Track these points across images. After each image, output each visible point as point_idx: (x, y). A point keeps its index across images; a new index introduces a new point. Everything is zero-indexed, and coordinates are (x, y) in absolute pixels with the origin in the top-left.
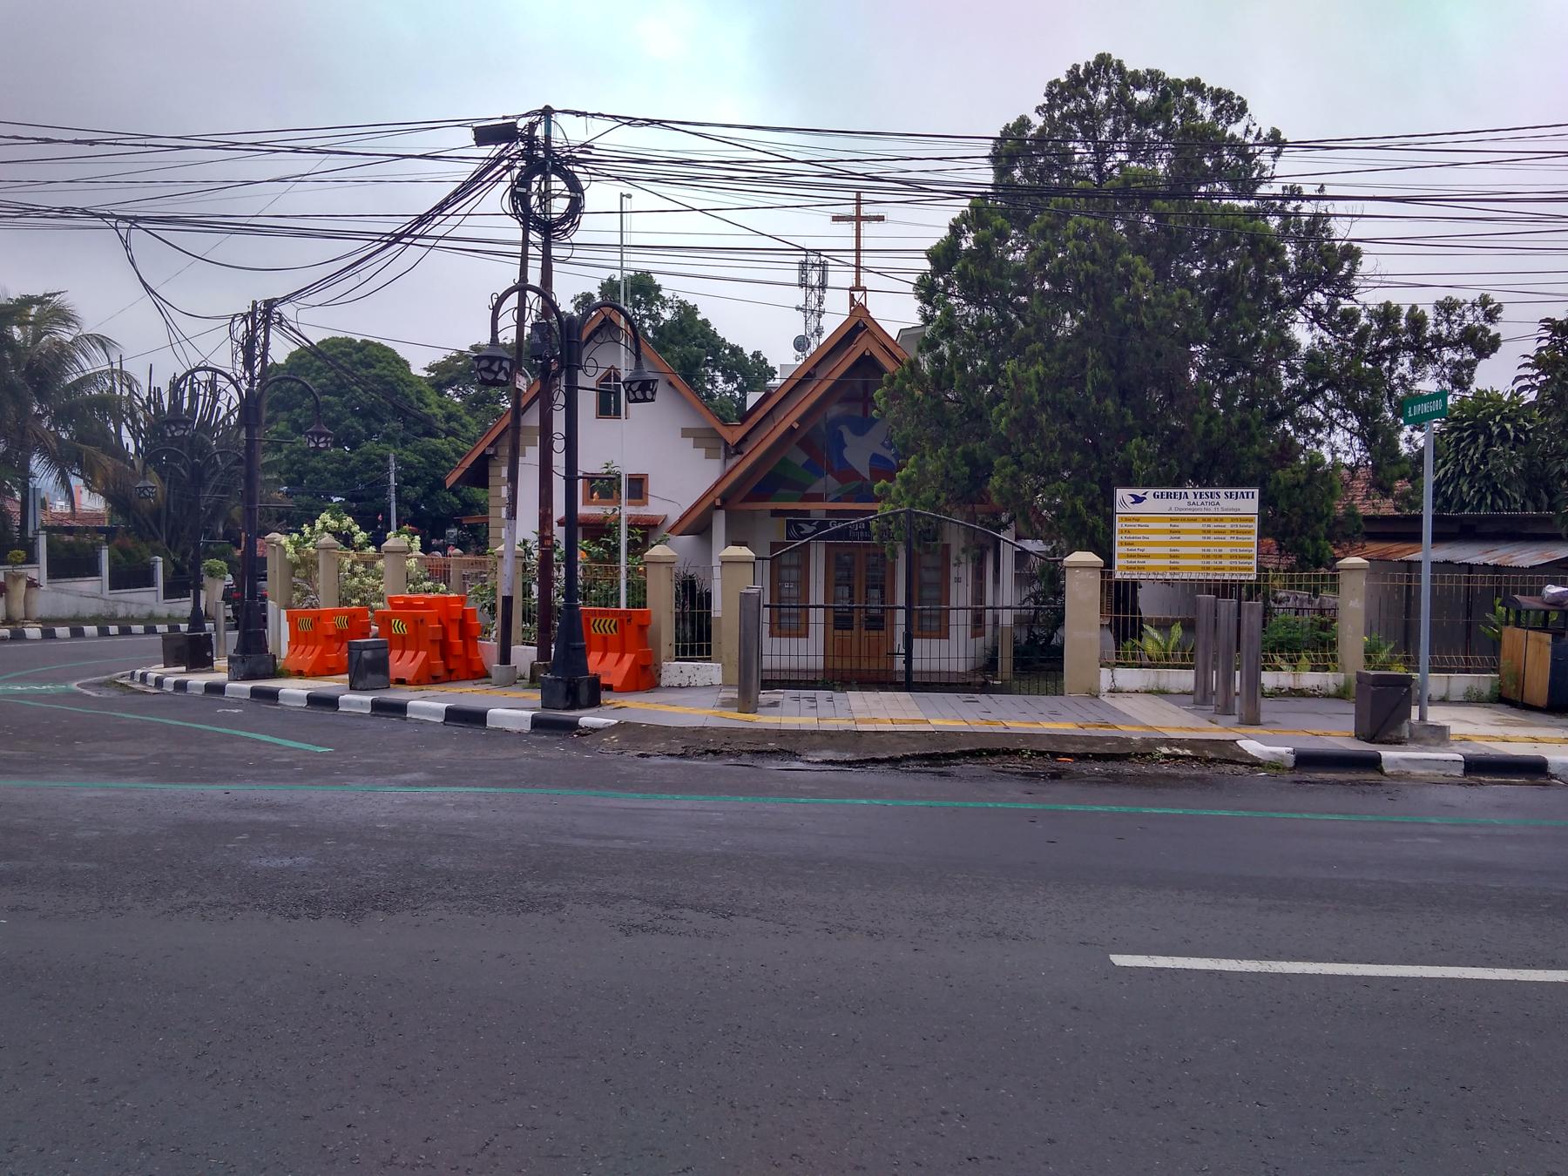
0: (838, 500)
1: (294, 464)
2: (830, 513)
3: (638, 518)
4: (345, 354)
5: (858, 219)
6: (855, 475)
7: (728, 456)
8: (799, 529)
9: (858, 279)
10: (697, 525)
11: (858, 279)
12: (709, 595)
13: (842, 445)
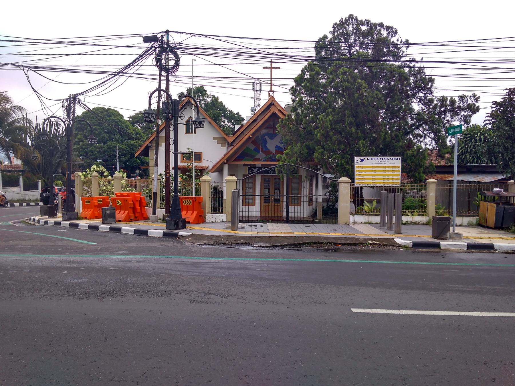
0: (265, 161)
2: (262, 165)
3: (199, 167)
4: (101, 112)
5: (271, 68)
6: (269, 152)
7: (229, 146)
9: (271, 88)
10: (219, 169)
11: (271, 88)
12: (222, 192)
13: (266, 142)
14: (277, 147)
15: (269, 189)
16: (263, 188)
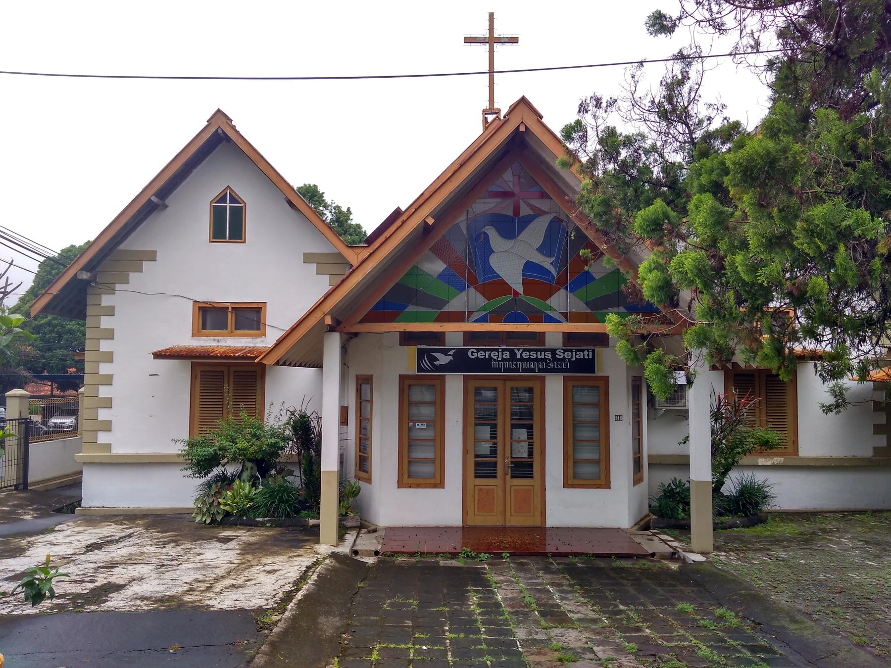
2: (471, 337)
5: (491, 40)
6: (501, 287)
8: (433, 359)
10: (303, 350)
14: (529, 266)
15: (494, 427)
16: (471, 420)
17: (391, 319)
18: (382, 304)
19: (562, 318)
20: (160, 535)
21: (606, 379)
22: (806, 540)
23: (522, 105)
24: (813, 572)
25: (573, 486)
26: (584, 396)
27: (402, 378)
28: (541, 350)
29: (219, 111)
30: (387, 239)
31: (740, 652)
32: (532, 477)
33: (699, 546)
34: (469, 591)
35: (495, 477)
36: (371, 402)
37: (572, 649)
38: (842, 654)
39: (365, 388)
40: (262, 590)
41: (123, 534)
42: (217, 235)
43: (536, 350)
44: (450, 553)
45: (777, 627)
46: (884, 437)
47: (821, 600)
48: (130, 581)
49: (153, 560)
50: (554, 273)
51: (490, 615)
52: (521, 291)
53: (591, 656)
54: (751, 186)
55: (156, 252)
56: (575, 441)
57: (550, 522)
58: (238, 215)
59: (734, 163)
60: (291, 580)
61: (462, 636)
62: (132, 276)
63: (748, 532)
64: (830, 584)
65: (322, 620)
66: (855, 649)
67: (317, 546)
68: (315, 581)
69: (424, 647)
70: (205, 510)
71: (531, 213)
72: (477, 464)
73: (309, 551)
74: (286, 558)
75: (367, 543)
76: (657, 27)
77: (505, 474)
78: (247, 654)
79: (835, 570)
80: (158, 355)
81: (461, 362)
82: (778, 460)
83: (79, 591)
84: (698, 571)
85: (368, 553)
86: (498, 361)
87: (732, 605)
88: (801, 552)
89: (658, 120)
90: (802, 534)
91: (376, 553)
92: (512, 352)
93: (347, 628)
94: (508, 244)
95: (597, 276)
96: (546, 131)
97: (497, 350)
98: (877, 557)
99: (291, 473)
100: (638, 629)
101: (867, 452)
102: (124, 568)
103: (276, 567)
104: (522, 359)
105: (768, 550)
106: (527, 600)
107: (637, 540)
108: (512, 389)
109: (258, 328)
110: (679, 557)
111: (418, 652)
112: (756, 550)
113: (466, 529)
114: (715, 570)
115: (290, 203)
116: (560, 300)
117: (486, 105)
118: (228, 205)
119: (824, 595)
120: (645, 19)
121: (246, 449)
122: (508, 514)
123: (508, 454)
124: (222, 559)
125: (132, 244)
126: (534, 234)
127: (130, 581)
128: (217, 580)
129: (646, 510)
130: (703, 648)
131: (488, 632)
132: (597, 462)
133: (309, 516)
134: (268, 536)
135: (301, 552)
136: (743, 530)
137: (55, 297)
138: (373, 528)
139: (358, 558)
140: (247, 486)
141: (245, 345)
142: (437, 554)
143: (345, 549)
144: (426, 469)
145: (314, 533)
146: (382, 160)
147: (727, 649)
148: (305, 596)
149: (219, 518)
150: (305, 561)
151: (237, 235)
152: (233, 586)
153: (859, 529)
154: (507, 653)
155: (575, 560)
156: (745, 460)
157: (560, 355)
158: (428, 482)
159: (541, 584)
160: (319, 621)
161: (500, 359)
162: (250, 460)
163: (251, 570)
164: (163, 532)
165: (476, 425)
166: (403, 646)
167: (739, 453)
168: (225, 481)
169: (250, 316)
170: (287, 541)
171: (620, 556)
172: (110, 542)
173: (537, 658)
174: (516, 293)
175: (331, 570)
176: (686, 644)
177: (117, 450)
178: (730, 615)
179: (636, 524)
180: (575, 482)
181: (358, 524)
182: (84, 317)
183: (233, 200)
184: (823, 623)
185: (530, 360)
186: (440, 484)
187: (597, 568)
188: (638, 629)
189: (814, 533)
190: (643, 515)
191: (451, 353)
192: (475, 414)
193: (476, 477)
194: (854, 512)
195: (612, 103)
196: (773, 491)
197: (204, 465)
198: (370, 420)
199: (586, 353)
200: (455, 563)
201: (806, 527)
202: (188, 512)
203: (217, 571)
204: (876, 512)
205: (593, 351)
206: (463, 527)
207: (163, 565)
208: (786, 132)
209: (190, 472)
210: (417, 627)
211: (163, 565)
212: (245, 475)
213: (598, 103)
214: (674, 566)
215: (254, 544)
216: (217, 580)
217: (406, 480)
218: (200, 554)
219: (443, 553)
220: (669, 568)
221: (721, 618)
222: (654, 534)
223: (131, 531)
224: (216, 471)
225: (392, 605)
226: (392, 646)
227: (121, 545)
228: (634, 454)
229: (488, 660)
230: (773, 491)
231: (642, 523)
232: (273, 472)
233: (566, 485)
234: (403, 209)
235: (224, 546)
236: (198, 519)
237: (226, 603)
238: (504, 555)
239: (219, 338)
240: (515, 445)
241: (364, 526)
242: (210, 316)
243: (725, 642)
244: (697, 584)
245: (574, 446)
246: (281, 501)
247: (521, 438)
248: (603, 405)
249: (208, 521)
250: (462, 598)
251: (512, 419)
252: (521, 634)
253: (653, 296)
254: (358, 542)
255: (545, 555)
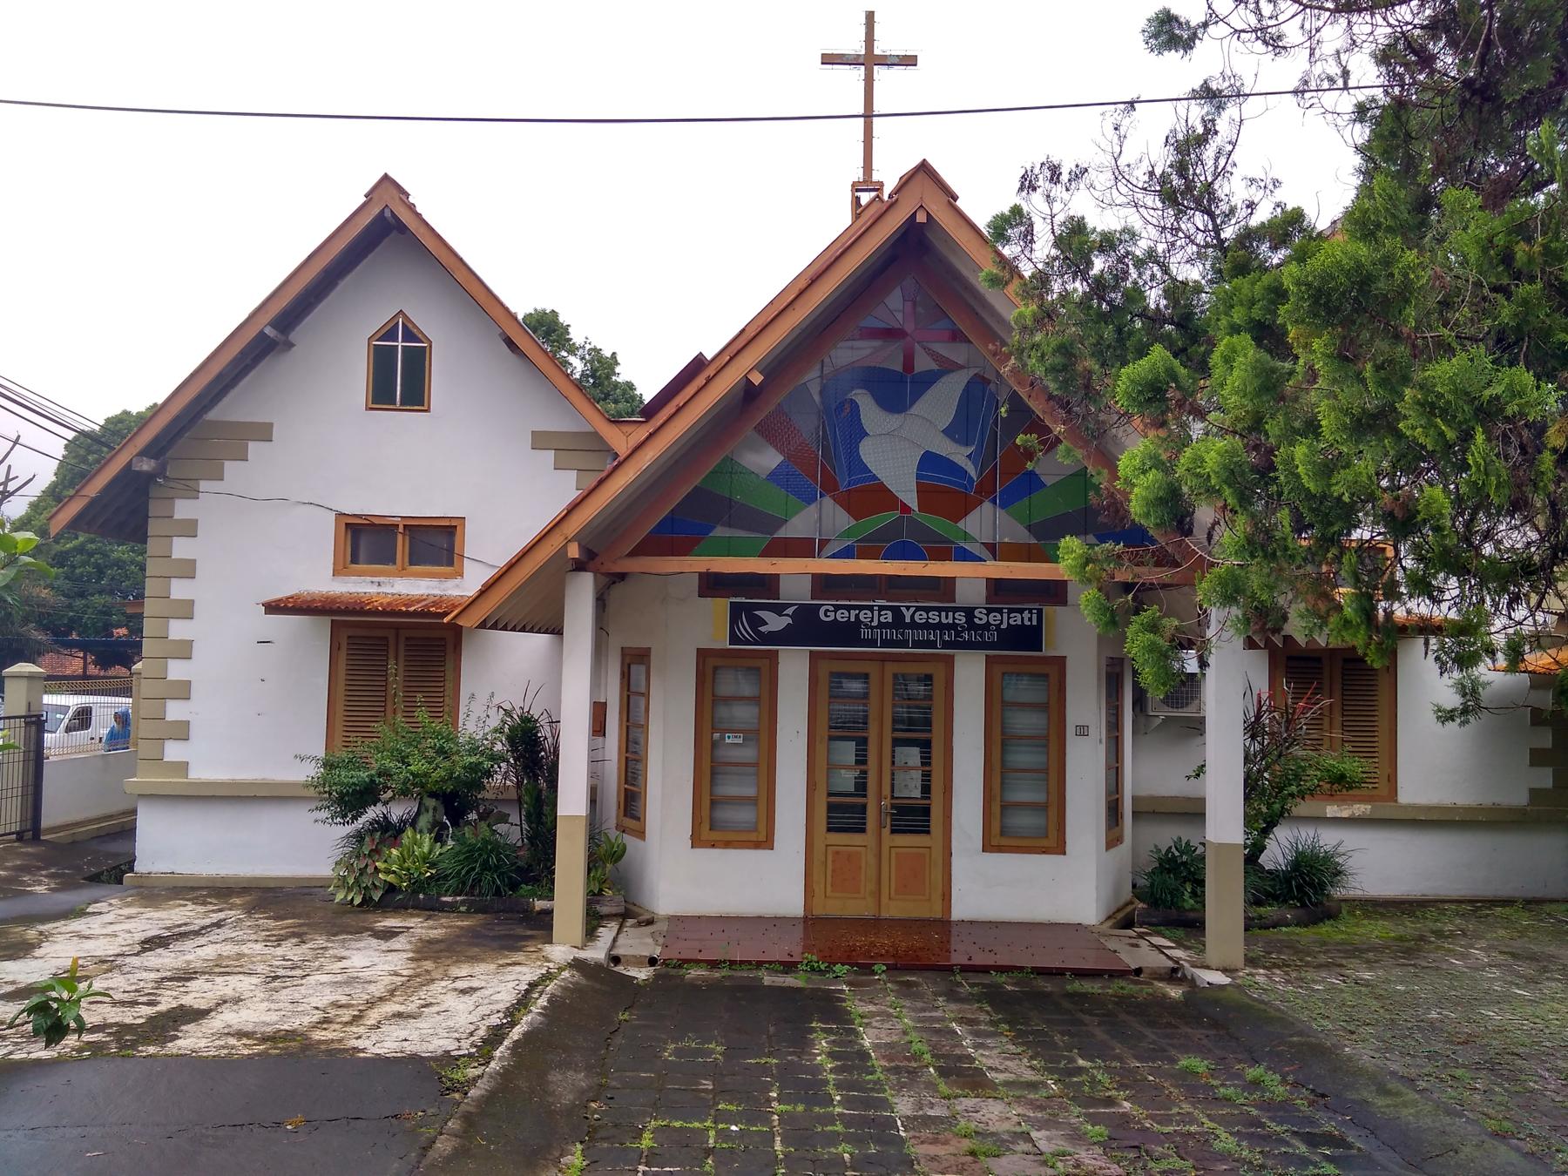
1: (91, 554)
2: (824, 585)
8: (757, 622)
10: (528, 602)
14: (930, 461)
15: (862, 743)
16: (823, 731)
17: (684, 550)
18: (669, 523)
19: (985, 553)
20: (272, 924)
21: (1061, 661)
22: (1408, 951)
23: (921, 175)
24: (1418, 1005)
25: (1000, 849)
26: (1022, 690)
27: (703, 654)
28: (947, 610)
29: (386, 177)
30: (679, 410)
31: (1288, 1144)
32: (928, 832)
33: (1220, 958)
34: (813, 1030)
35: (863, 831)
36: (646, 695)
37: (993, 1134)
38: (1467, 1150)
39: (638, 671)
40: (451, 1023)
41: (207, 921)
42: (381, 396)
43: (939, 610)
44: (781, 963)
45: (1353, 1101)
46: (1549, 771)
47: (1432, 1056)
48: (218, 1005)
49: (260, 968)
50: (972, 472)
51: (851, 1073)
52: (914, 505)
53: (1027, 1147)
54: (1327, 324)
55: (271, 425)
56: (1006, 769)
57: (958, 913)
58: (418, 363)
59: (1298, 283)
60: (502, 1006)
61: (800, 1108)
62: (229, 466)
63: (1306, 935)
64: (1449, 1029)
65: (555, 1077)
66: (1490, 1143)
67: (548, 948)
68: (544, 1008)
69: (734, 1128)
70: (351, 881)
71: (934, 366)
72: (831, 808)
73: (534, 956)
74: (493, 967)
75: (637, 943)
76: (1163, 38)
77: (881, 826)
78: (422, 1134)
79: (1458, 1004)
80: (273, 608)
81: (806, 629)
82: (1360, 809)
83: (128, 1021)
84: (1216, 1002)
85: (638, 961)
86: (872, 628)
87: (1276, 1061)
88: (1398, 972)
89: (1160, 205)
90: (1401, 939)
91: (652, 961)
92: (896, 611)
93: (598, 1092)
94: (894, 421)
95: (1049, 481)
96: (963, 223)
97: (871, 608)
98: (1531, 981)
99: (504, 818)
100: (1110, 1102)
101: (1520, 799)
102: (207, 981)
103: (475, 984)
104: (914, 625)
105: (1341, 966)
106: (916, 1047)
107: (1112, 944)
108: (895, 676)
109: (451, 563)
110: (1184, 975)
111: (723, 1135)
112: (1320, 966)
113: (811, 922)
114: (1247, 1000)
115: (510, 343)
116: (982, 522)
117: (859, 175)
118: (400, 344)
119: (1438, 1047)
120: (1143, 24)
121: (426, 775)
122: (885, 900)
123: (886, 791)
124: (380, 967)
125: (230, 410)
126: (940, 404)
127: (218, 1005)
128: (371, 1003)
129: (1127, 893)
130: (1224, 1136)
131: (846, 1102)
132: (1041, 808)
133: (534, 894)
134: (461, 928)
135: (519, 957)
136: (1298, 930)
137: (93, 503)
138: (646, 917)
139: (620, 969)
140: (427, 841)
141: (426, 592)
142: (759, 964)
143: (596, 953)
144: (745, 815)
145: (543, 925)
146: (673, 269)
147: (1266, 1138)
148: (526, 1035)
149: (377, 896)
150: (527, 973)
151: (416, 397)
152: (399, 1015)
153: (1502, 932)
154: (878, 1141)
155: (1002, 978)
156: (1303, 808)
157: (981, 618)
158: (744, 837)
159: (938, 1020)
160: (550, 1078)
161: (875, 623)
162: (432, 795)
163: (432, 987)
164: (276, 918)
165: (831, 738)
166: (697, 1125)
167: (1292, 795)
168: (388, 831)
169: (435, 541)
170: (494, 938)
171: (1081, 974)
172: (183, 936)
173: (933, 1150)
174: (906, 509)
175: (572, 991)
176: (1193, 1129)
177: (198, 773)
178: (1272, 1079)
179: (1109, 918)
180: (1005, 841)
181: (621, 910)
182: (143, 539)
183: (410, 335)
184: (1435, 1096)
185: (927, 626)
186: (767, 843)
187: (1040, 994)
188: (1110, 1102)
189: (1422, 938)
190: (1122, 902)
191: (790, 611)
192: (830, 719)
193: (829, 830)
194: (1493, 903)
195: (1080, 173)
196: (1350, 864)
197: (351, 801)
198: (645, 727)
199: (1026, 615)
200: (789, 981)
201: (1409, 927)
202: (322, 884)
203: (372, 988)
204: (1531, 904)
205: (1040, 612)
206: (805, 918)
207: (277, 977)
208: (1390, 229)
209: (325, 814)
210: (721, 1092)
211: (276, 978)
212: (424, 821)
213: (1055, 173)
214: (1175, 992)
215: (437, 941)
216: (371, 1003)
217: (706, 833)
218: (341, 958)
219: (770, 963)
220: (1165, 996)
221: (1256, 1084)
222: (1141, 936)
223: (221, 915)
224: (372, 813)
225: (678, 1053)
226: (677, 1124)
227: (202, 940)
228: (1108, 794)
229: (846, 1152)
230: (1350, 862)
231: (1120, 915)
232: (473, 816)
233: (988, 847)
234: (709, 358)
235: (385, 945)
236: (340, 896)
237: (386, 1045)
238: (876, 968)
239: (382, 579)
240: (899, 776)
241: (631, 914)
242: (366, 539)
243: (1262, 1125)
244: (1215, 1024)
245: (1003, 779)
246: (486, 866)
247: (911, 763)
248: (1055, 707)
249: (357, 901)
250: (802, 1043)
251: (894, 730)
252: (903, 1106)
253: (1147, 515)
254: (621, 940)
255: (949, 969)
